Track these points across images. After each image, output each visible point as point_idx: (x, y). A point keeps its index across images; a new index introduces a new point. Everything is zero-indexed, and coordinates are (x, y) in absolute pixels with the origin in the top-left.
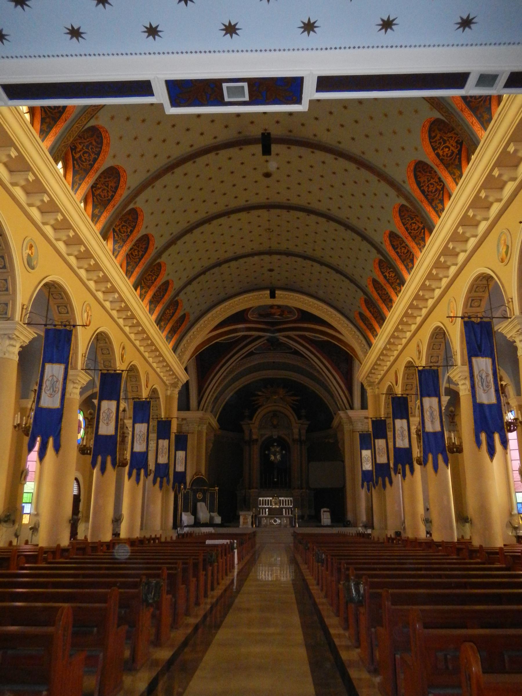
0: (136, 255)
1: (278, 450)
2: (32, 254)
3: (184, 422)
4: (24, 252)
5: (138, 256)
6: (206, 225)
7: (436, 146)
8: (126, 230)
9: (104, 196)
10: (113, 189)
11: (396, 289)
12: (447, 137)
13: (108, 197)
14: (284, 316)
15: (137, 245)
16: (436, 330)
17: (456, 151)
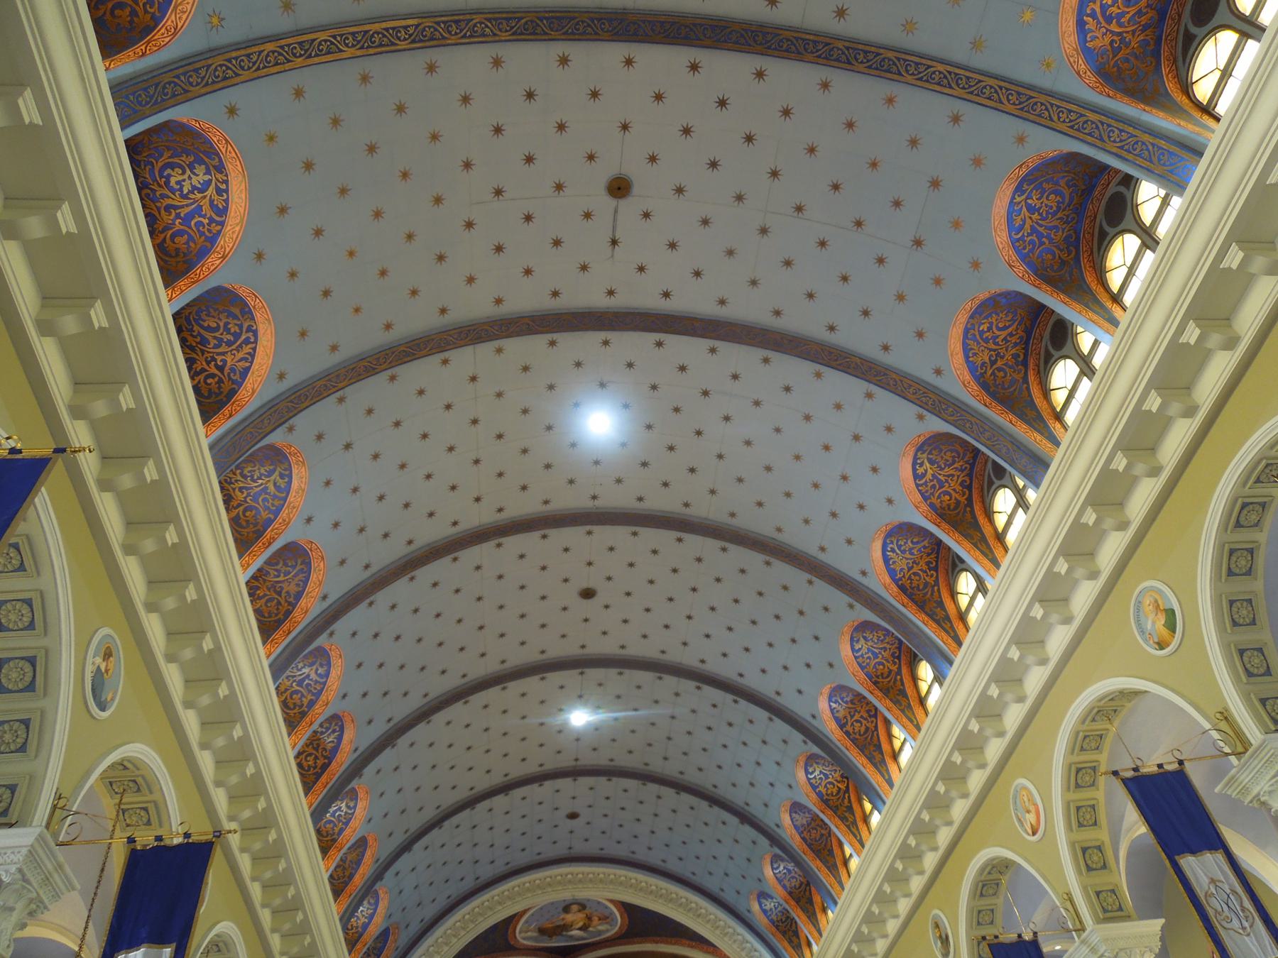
0: (309, 766)
2: (107, 671)
4: (90, 660)
5: (315, 768)
6: (459, 706)
7: (927, 491)
8: (298, 702)
9: (269, 613)
10: (291, 600)
11: (847, 820)
12: (944, 475)
13: (276, 615)
14: (591, 929)
15: (315, 743)
16: (981, 874)
17: (962, 499)
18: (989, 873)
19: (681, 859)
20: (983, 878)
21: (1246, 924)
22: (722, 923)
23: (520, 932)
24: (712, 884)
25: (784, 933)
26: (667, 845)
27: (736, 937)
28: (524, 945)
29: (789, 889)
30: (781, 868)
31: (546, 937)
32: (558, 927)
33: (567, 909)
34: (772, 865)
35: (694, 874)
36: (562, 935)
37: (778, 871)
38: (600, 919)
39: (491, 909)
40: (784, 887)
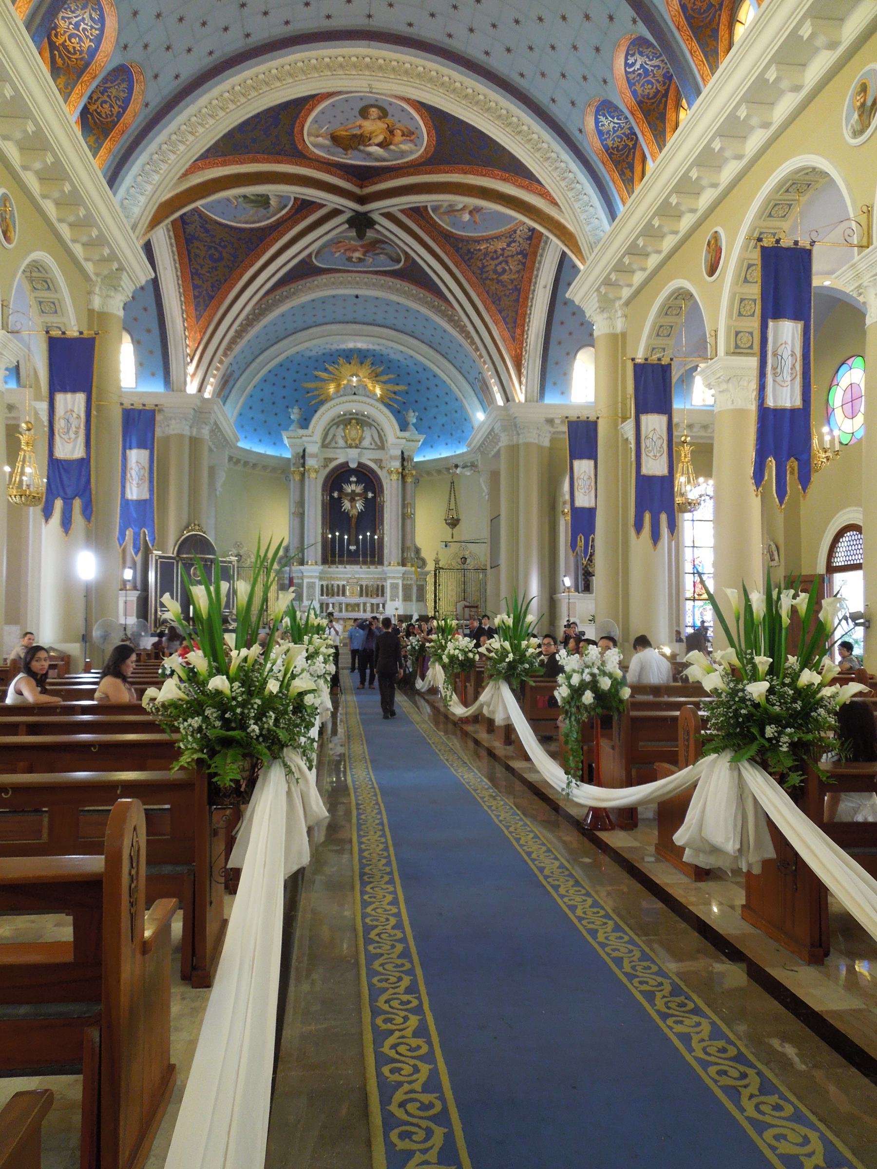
1: (359, 489)
14: (392, 147)
19: (508, 50)
22: (545, 145)
23: (309, 135)
24: (540, 92)
25: (617, 163)
26: (494, 26)
27: (558, 164)
29: (640, 98)
30: (637, 66)
31: (340, 150)
32: (354, 136)
33: (364, 113)
34: (626, 59)
35: (522, 75)
36: (360, 151)
37: (631, 70)
38: (403, 135)
39: (267, 84)
40: (634, 93)
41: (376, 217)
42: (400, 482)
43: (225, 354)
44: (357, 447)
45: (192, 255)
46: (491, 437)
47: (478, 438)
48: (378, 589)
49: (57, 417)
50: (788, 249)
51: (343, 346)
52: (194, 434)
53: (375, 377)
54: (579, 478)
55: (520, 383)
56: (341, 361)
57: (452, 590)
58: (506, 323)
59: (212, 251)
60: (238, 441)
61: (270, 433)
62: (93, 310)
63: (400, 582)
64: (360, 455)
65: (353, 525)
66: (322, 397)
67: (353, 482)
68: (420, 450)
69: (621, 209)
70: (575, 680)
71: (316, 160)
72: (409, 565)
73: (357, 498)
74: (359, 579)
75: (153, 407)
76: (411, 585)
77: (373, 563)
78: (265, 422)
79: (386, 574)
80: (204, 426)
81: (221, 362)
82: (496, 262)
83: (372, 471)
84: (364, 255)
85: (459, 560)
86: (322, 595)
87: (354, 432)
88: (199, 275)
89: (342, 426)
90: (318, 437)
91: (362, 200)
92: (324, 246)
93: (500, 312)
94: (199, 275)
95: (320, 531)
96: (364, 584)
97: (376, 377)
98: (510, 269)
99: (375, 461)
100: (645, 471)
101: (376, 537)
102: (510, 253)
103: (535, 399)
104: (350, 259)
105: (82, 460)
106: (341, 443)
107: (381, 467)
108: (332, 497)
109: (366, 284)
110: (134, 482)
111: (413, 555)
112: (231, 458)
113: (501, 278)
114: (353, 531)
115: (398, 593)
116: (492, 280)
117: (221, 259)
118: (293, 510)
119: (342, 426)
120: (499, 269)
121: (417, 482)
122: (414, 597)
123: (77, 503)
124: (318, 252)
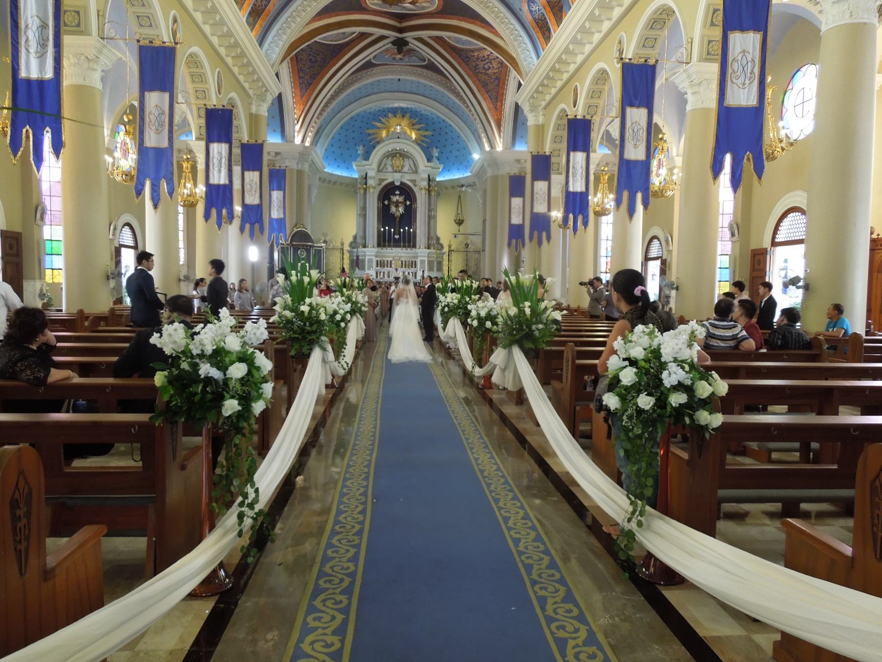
1: (401, 199)
3: (278, 158)
14: (417, 4)
16: (655, 14)
18: (661, 14)
20: (655, 17)
21: (747, 82)
25: (541, 28)
28: (371, 7)
31: (388, 5)
41: (409, 40)
42: (427, 195)
43: (318, 118)
44: (399, 172)
45: (299, 60)
46: (482, 170)
47: (476, 168)
48: (412, 263)
49: (245, 184)
50: (580, 120)
51: (391, 106)
52: (300, 168)
53: (412, 126)
54: (514, 208)
55: (500, 136)
56: (390, 115)
57: (459, 264)
58: (491, 99)
59: (311, 57)
60: (325, 168)
61: (344, 162)
62: (252, 114)
63: (426, 259)
64: (402, 177)
65: (397, 222)
66: (378, 139)
67: (397, 194)
68: (440, 174)
69: (542, 53)
70: (443, 304)
71: (373, 11)
72: (432, 248)
73: (400, 205)
74: (401, 257)
75: (285, 168)
76: (433, 261)
77: (409, 246)
78: (342, 154)
79: (417, 254)
80: (305, 163)
81: (315, 123)
82: (485, 62)
83: (409, 187)
84: (404, 56)
85: (464, 246)
86: (377, 267)
87: (398, 162)
88: (302, 71)
89: (390, 158)
90: (375, 166)
91: (401, 30)
92: (380, 53)
93: (487, 92)
94: (302, 71)
95: (376, 226)
96: (403, 260)
97: (414, 125)
98: (493, 67)
99: (411, 181)
100: (535, 210)
101: (411, 230)
102: (493, 58)
103: (509, 147)
104: (394, 59)
105: (258, 205)
106: (390, 169)
107: (415, 185)
108: (384, 204)
109: (404, 72)
110: (276, 209)
111: (435, 242)
112: (320, 179)
113: (488, 72)
114: (397, 226)
115: (425, 266)
116: (482, 73)
117: (316, 61)
118: (359, 213)
119: (390, 158)
120: (486, 66)
121: (438, 194)
122: (435, 269)
123: (257, 226)
124: (374, 57)
